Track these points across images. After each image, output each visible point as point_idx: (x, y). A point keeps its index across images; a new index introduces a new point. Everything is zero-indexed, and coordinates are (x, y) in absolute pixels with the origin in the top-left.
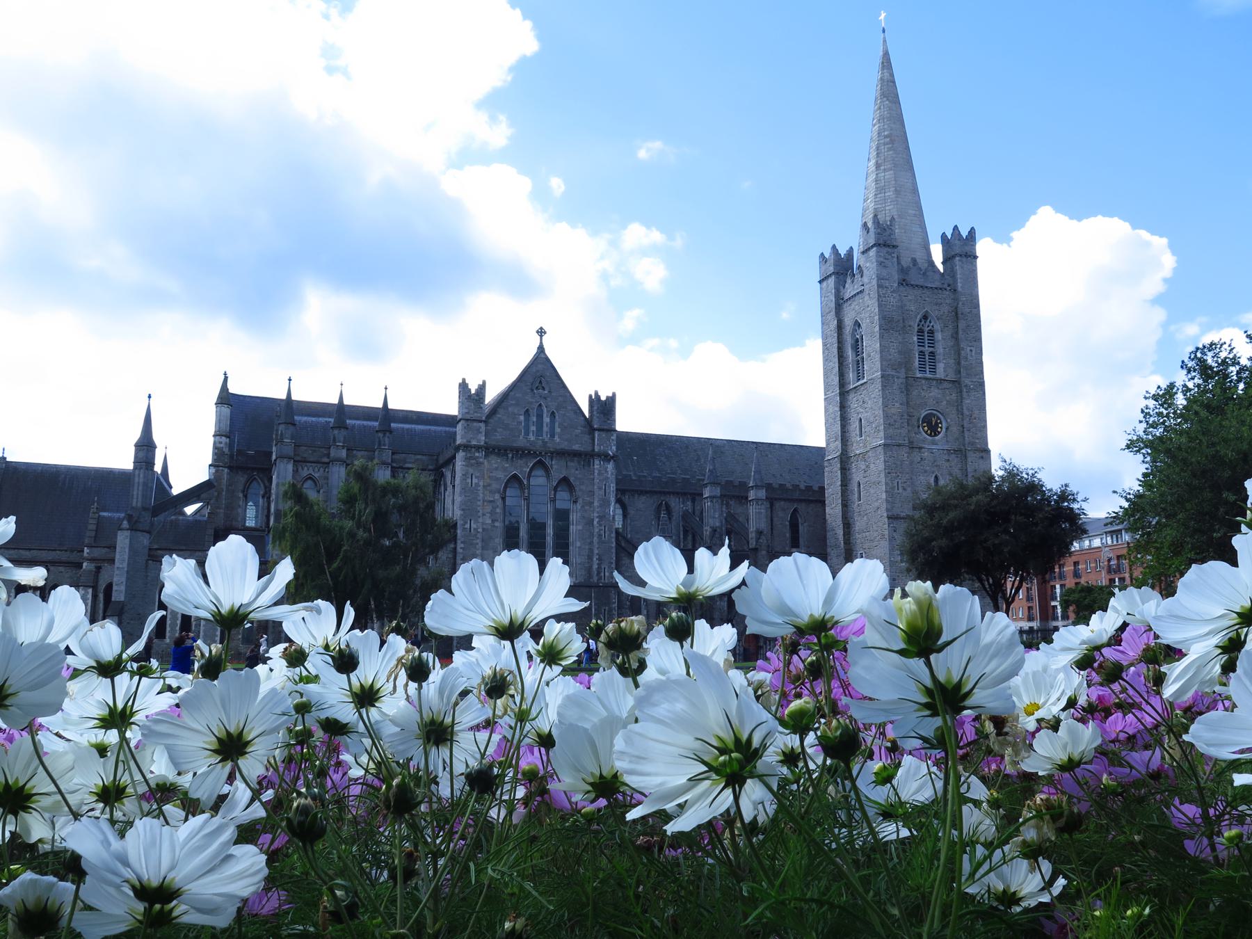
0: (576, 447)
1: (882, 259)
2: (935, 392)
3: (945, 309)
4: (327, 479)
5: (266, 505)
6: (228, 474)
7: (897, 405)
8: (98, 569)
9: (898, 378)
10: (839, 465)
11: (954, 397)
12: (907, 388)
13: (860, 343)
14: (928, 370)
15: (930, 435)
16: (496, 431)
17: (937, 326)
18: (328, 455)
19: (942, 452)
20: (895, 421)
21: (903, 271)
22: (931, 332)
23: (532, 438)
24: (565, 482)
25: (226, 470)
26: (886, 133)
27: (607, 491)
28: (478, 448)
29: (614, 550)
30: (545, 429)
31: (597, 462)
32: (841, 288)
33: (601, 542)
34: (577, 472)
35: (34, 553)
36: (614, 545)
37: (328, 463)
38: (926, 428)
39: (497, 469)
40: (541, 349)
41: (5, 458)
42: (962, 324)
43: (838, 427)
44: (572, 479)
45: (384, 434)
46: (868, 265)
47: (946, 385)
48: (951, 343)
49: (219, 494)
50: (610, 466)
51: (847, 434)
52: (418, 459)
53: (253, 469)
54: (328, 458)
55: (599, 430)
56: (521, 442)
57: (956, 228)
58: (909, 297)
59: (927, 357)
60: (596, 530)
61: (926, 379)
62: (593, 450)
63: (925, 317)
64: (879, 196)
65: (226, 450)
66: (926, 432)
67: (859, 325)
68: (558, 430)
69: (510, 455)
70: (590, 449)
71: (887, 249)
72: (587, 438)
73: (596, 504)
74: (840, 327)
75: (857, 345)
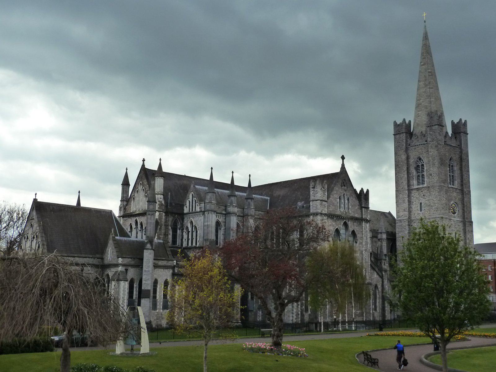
0: (356, 216)
1: (439, 132)
2: (455, 194)
3: (458, 156)
4: (225, 222)
5: (181, 234)
6: (165, 216)
7: (445, 199)
8: (126, 270)
9: (445, 187)
10: (407, 223)
11: (460, 197)
12: (447, 192)
13: (420, 167)
14: (452, 184)
15: (453, 214)
16: (330, 206)
17: (455, 164)
18: (226, 210)
19: (458, 222)
20: (444, 207)
21: (445, 137)
22: (452, 166)
23: (342, 210)
24: (354, 233)
25: (164, 214)
26: (429, 70)
27: (367, 237)
28: (325, 215)
29: (370, 267)
30: (347, 206)
31: (364, 223)
32: (408, 140)
33: (366, 262)
34: (357, 228)
35: (77, 259)
36: (370, 264)
37: (225, 214)
38: (452, 210)
39: (330, 225)
40: (343, 165)
41: (37, 199)
42: (464, 164)
43: (406, 205)
44: (355, 231)
45: (252, 200)
46: (431, 133)
47: (458, 191)
48: (459, 172)
49: (161, 227)
50: (368, 225)
51: (411, 209)
52: (260, 214)
53: (176, 214)
54: (226, 211)
55: (364, 207)
56: (338, 213)
57: (461, 120)
58: (447, 150)
59: (451, 178)
60: (364, 256)
61: (452, 188)
62: (362, 217)
63: (450, 159)
64: (427, 99)
65: (163, 202)
66: (452, 212)
67: (420, 159)
68: (350, 207)
69: (335, 219)
70: (361, 216)
71: (441, 127)
72: (359, 211)
73: (364, 244)
74: (408, 158)
75: (419, 168)
